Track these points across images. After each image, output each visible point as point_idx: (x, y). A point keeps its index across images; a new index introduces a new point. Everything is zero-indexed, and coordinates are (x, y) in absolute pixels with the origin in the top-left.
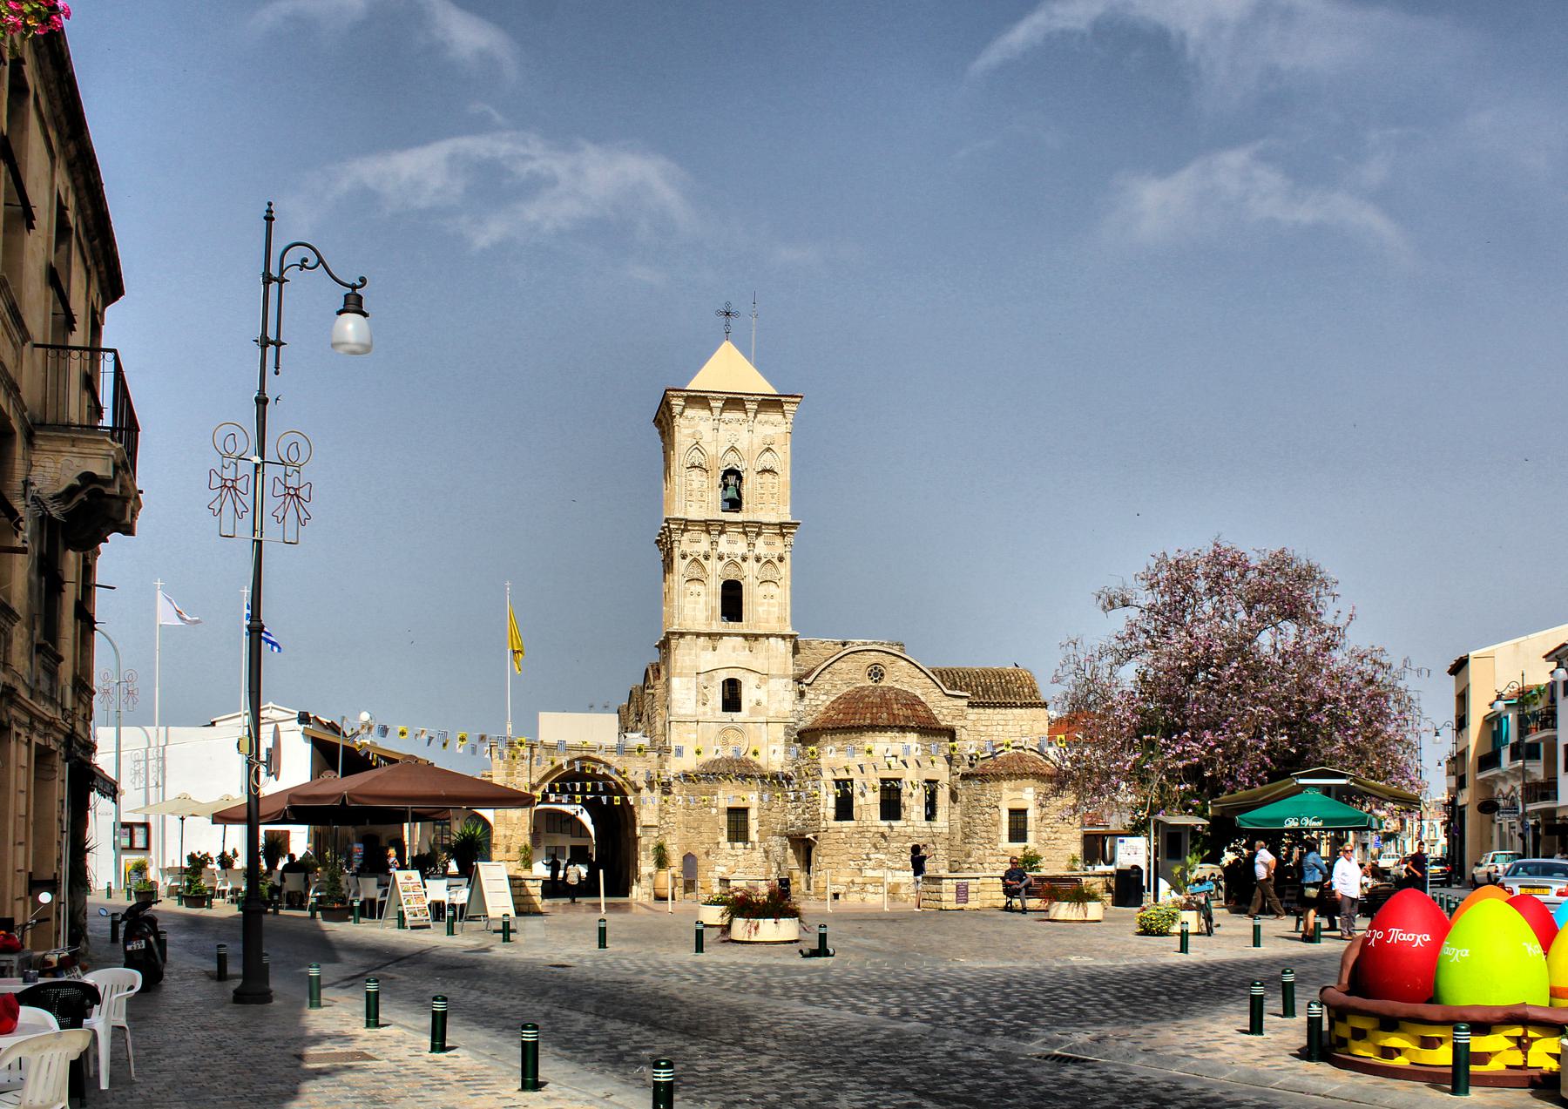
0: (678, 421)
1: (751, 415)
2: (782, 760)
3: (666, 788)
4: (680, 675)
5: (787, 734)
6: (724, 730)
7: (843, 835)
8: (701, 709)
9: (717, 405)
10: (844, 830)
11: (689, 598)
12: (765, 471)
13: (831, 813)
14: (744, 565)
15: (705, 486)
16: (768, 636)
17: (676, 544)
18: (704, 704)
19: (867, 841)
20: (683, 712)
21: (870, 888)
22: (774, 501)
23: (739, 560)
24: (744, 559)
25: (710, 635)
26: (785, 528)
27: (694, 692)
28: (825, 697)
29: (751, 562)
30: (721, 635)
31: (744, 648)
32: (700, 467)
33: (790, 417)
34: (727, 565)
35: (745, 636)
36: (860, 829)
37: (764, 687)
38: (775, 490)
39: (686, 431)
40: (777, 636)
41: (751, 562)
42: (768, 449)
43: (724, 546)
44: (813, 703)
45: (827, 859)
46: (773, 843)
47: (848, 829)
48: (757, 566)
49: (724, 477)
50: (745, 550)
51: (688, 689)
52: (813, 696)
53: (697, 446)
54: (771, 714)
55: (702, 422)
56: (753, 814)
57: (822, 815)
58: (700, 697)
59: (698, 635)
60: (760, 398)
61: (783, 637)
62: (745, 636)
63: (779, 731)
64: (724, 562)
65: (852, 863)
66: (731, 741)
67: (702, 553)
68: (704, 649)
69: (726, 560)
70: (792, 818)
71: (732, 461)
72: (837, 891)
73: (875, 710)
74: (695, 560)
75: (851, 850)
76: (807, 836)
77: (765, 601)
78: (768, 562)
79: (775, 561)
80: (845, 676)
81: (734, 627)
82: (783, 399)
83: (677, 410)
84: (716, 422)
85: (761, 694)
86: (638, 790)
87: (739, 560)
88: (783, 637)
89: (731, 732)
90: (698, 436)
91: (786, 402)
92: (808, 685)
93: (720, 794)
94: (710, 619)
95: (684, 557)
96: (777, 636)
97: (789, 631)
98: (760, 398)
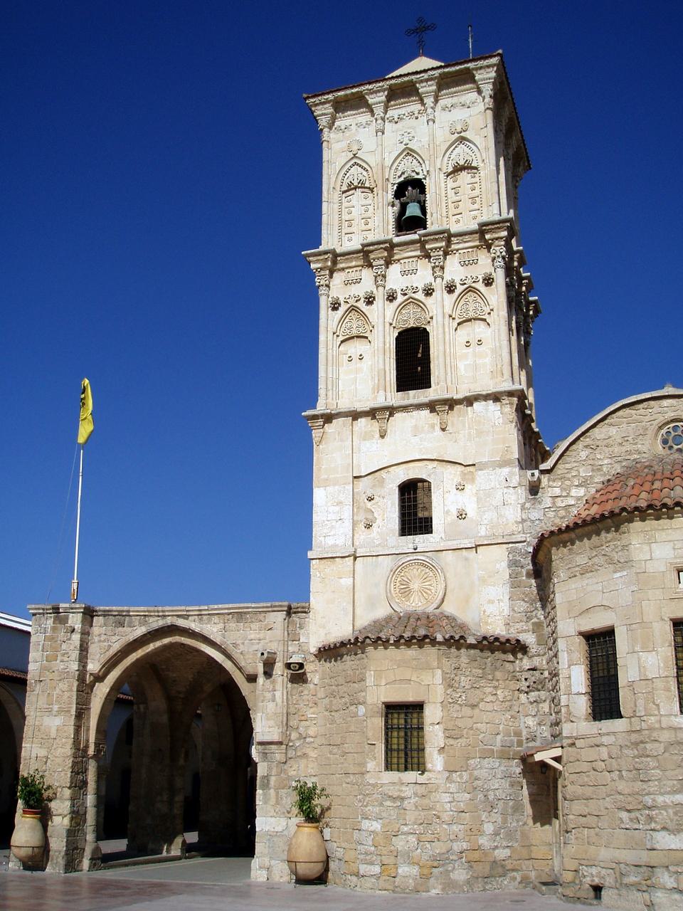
0: (326, 135)
1: (429, 101)
2: (506, 612)
3: (298, 675)
4: (326, 484)
5: (513, 564)
6: (402, 567)
7: (604, 753)
8: (362, 536)
9: (377, 99)
10: (605, 740)
11: (345, 367)
12: (458, 169)
13: (582, 705)
14: (429, 301)
15: (371, 208)
16: (469, 401)
17: (322, 291)
18: (368, 526)
19: (653, 763)
20: (330, 541)
21: (667, 880)
22: (476, 206)
23: (420, 296)
24: (429, 292)
25: (372, 413)
26: (488, 231)
27: (347, 513)
28: (581, 492)
29: (440, 293)
30: (392, 410)
31: (433, 426)
32: (361, 186)
33: (488, 89)
34: (404, 306)
35: (432, 406)
36: (634, 737)
37: (468, 487)
38: (476, 192)
39: (336, 147)
40: (486, 397)
41: (440, 293)
42: (462, 140)
43: (395, 278)
44: (560, 503)
45: (577, 807)
46: (482, 773)
47: (611, 739)
48: (449, 300)
49: (400, 191)
50: (430, 279)
51: (339, 503)
52: (557, 491)
53: (355, 160)
54: (483, 533)
55: (361, 130)
56: (431, 714)
57: (563, 710)
58: (361, 517)
59: (356, 415)
60: (436, 73)
61: (496, 397)
62: (432, 406)
63: (497, 559)
64: (396, 303)
65: (624, 815)
66: (415, 585)
67: (362, 295)
68: (366, 437)
69: (400, 299)
70: (531, 722)
71: (409, 168)
72: (597, 881)
73: (657, 485)
74: (353, 309)
75: (621, 786)
76: (538, 757)
77: (470, 350)
78: (470, 289)
79: (480, 286)
80: (617, 449)
81: (415, 396)
82: (471, 65)
83: (323, 122)
84: (380, 121)
85: (468, 501)
86: (252, 679)
87: (420, 296)
88: (496, 397)
89: (415, 572)
90: (355, 148)
91: (477, 69)
92: (543, 472)
93: (370, 680)
94: (376, 390)
95: (335, 306)
96: (486, 397)
97: (507, 386)
98: (436, 73)
